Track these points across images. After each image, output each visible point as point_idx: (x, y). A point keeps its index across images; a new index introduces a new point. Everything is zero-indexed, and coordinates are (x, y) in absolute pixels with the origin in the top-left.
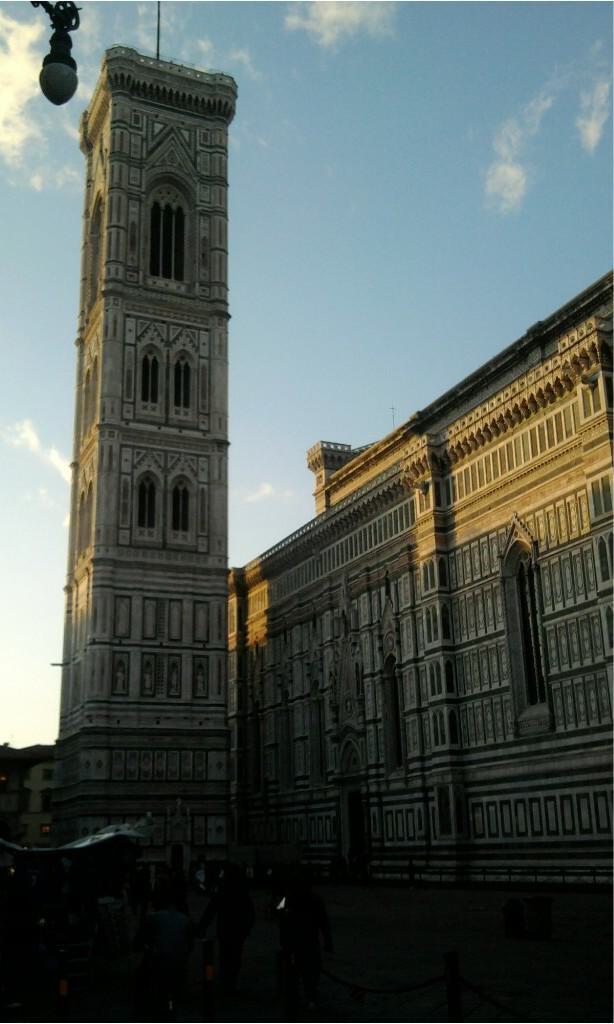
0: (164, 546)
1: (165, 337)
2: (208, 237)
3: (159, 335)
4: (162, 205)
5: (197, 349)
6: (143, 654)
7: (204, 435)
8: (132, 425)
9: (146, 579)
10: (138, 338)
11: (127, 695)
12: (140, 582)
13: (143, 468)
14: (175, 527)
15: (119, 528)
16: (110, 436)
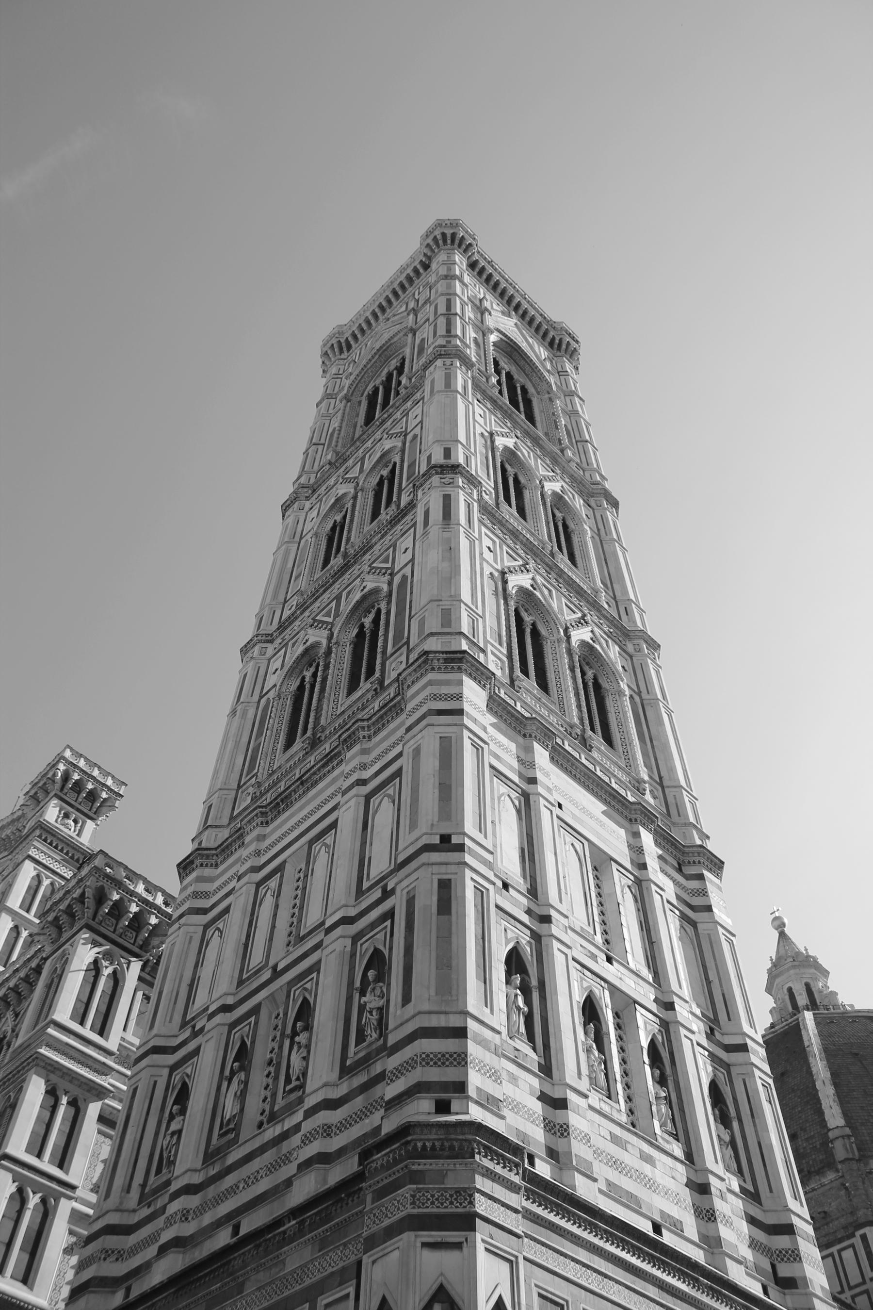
9: (268, 842)
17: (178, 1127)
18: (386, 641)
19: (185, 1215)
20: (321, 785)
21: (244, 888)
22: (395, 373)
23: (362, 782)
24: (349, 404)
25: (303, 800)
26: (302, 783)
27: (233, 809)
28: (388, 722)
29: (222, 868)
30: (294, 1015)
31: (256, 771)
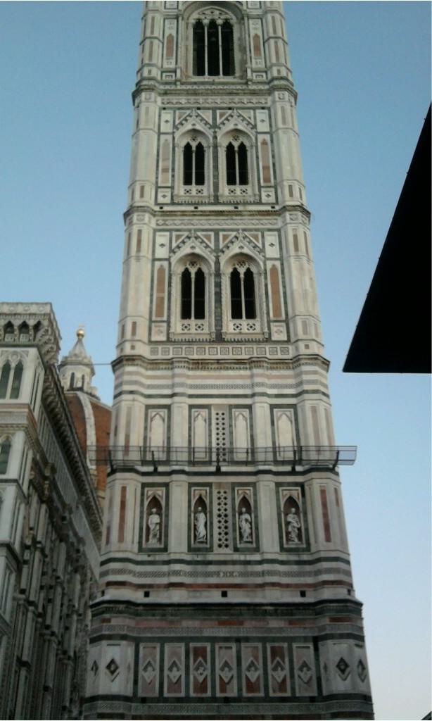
0: (219, 338)
1: (211, 122)
2: (260, 34)
3: (201, 120)
4: (206, 22)
5: (255, 127)
6: (191, 485)
7: (273, 207)
8: (166, 208)
9: (190, 382)
10: (175, 127)
11: (165, 549)
12: (182, 385)
13: (186, 250)
14: (236, 314)
15: (151, 321)
16: (138, 220)
17: (158, 521)
18: (268, 306)
19: (186, 574)
20: (231, 373)
21: (183, 405)
22: (220, 28)
23: (269, 396)
24: (183, 22)
25: (217, 373)
26: (218, 363)
27: (150, 334)
28: (280, 368)
29: (150, 373)
30: (239, 501)
31: (165, 318)
